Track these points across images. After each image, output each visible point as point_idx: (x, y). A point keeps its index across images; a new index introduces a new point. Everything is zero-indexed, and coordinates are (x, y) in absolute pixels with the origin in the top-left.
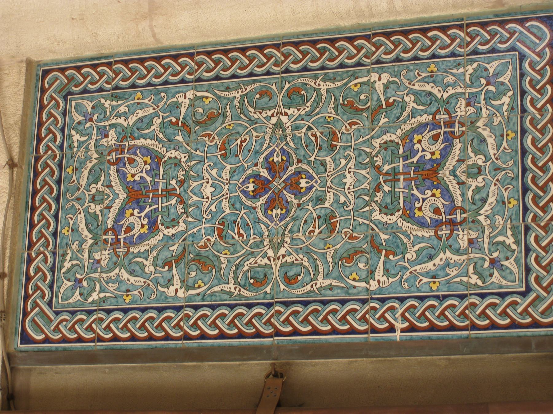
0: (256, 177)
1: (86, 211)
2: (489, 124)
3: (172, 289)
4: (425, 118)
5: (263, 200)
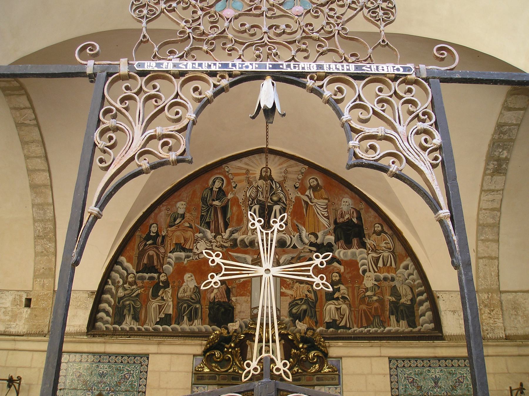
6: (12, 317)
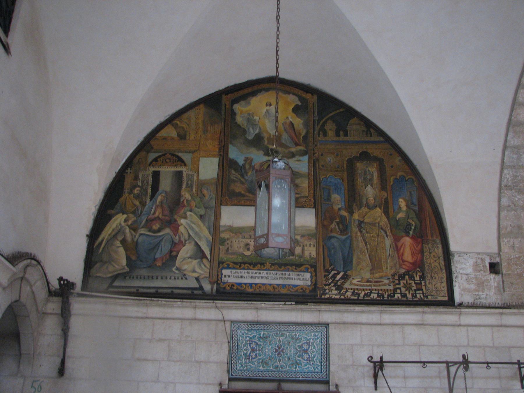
0: (276, 349)
1: (243, 352)
2: (316, 344)
3: (260, 368)
4: (305, 342)
5: (277, 353)
6: (478, 285)
